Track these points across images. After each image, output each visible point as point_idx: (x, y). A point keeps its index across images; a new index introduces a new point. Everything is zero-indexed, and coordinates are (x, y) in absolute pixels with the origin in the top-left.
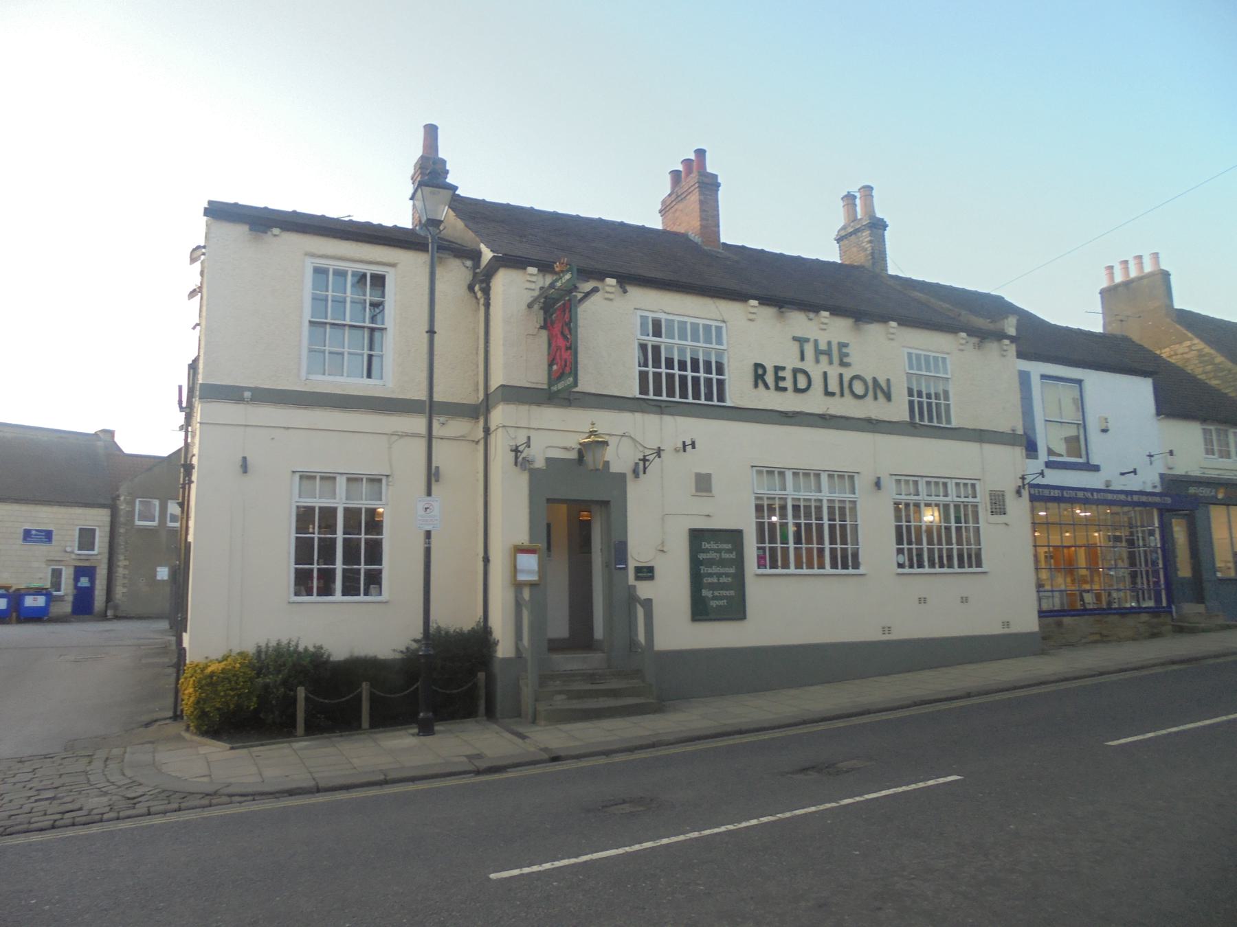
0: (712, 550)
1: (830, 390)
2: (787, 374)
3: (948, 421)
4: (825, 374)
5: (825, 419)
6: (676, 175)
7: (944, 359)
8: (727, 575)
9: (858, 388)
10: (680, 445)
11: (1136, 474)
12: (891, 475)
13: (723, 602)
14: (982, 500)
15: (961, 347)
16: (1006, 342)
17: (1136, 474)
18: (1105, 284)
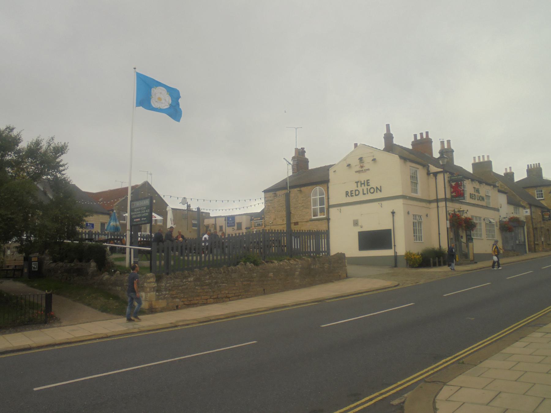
2: (473, 195)
6: (415, 136)
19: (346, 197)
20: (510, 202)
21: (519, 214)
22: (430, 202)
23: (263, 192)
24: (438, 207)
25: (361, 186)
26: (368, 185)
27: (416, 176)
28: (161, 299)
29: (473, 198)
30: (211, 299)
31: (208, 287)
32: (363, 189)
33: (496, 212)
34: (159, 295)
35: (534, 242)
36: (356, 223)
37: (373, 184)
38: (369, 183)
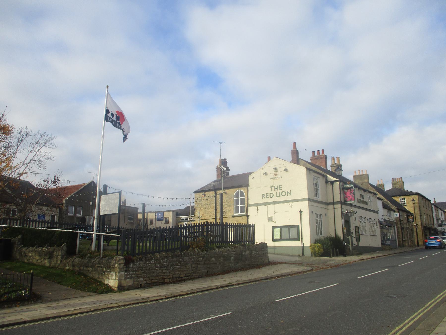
6: (314, 152)
19: (263, 198)
20: (385, 206)
22: (328, 204)
23: (193, 192)
24: (334, 208)
25: (275, 190)
26: (280, 190)
27: (317, 184)
28: (129, 278)
29: (360, 202)
30: (167, 279)
31: (165, 268)
32: (276, 193)
33: (376, 214)
34: (127, 275)
35: (402, 239)
36: (270, 219)
37: (284, 189)
38: (281, 188)
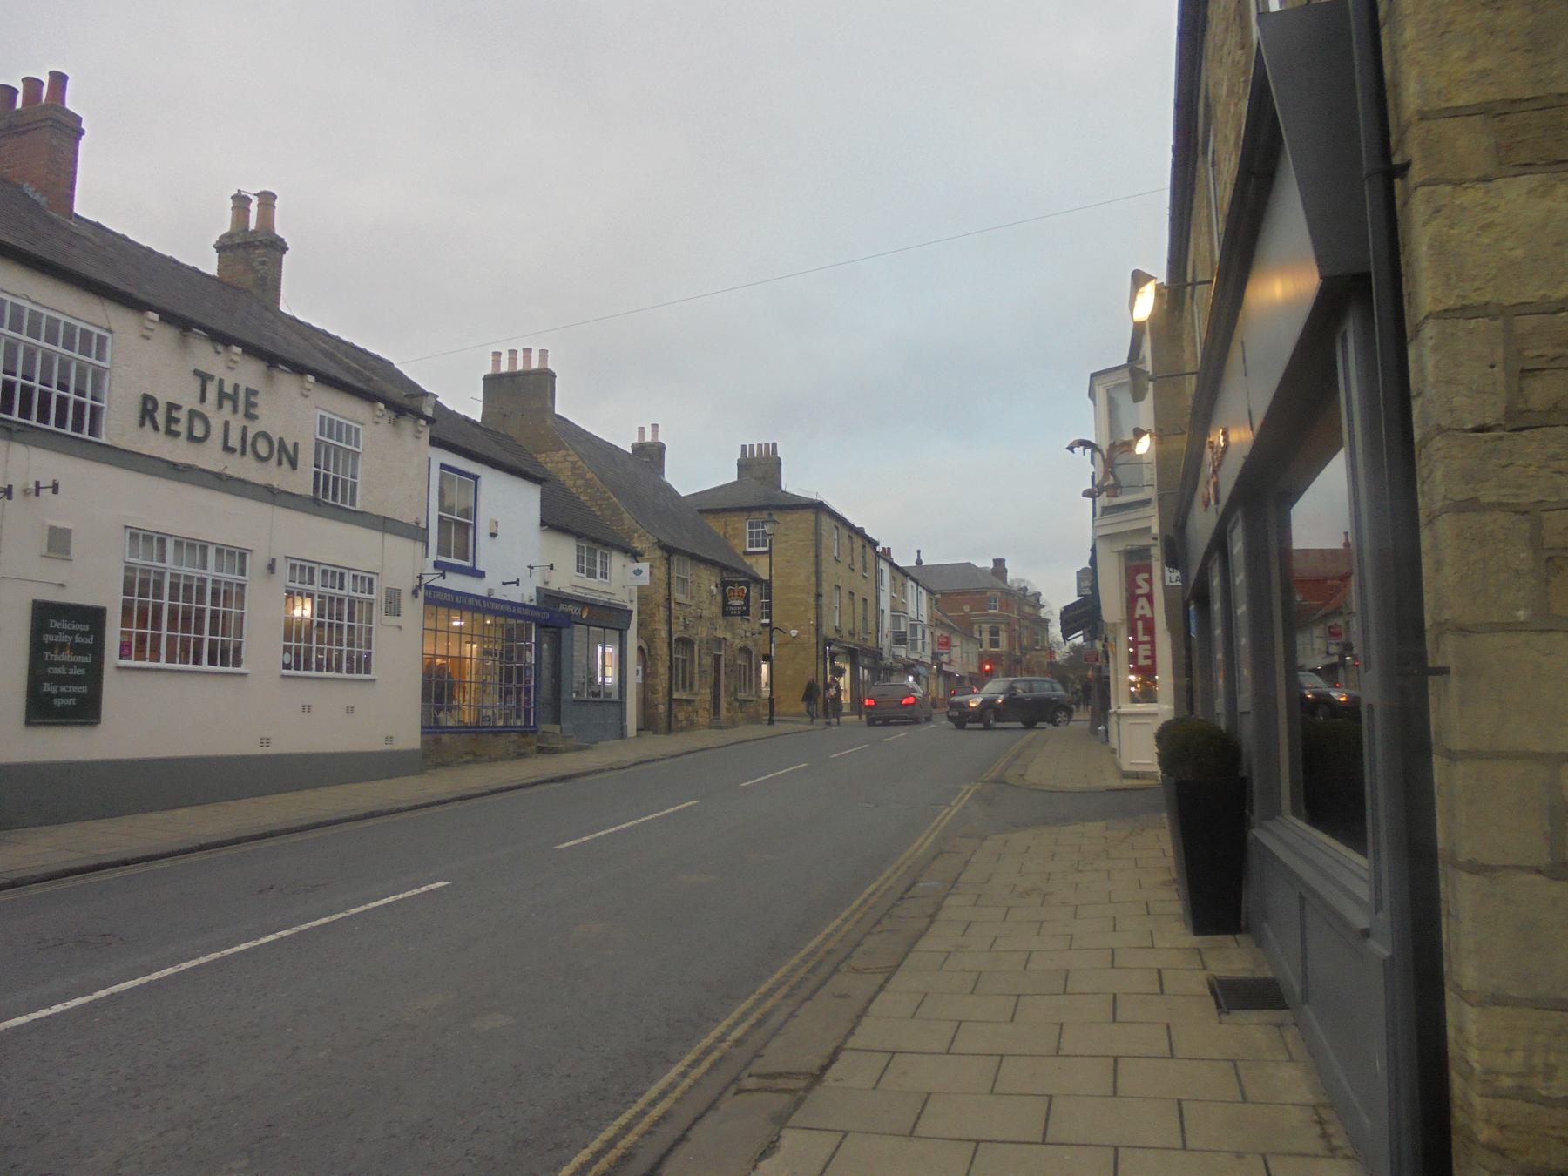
0: (62, 630)
1: (230, 444)
2: (182, 415)
3: (353, 503)
4: (227, 424)
5: (221, 479)
7: (357, 430)
8: (80, 665)
9: (263, 449)
10: (32, 486)
11: (518, 585)
12: (287, 557)
13: (71, 701)
14: (378, 595)
15: (376, 419)
16: (423, 422)
17: (518, 585)
18: (489, 370)
20: (552, 522)
21: (604, 575)
35: (670, 693)
